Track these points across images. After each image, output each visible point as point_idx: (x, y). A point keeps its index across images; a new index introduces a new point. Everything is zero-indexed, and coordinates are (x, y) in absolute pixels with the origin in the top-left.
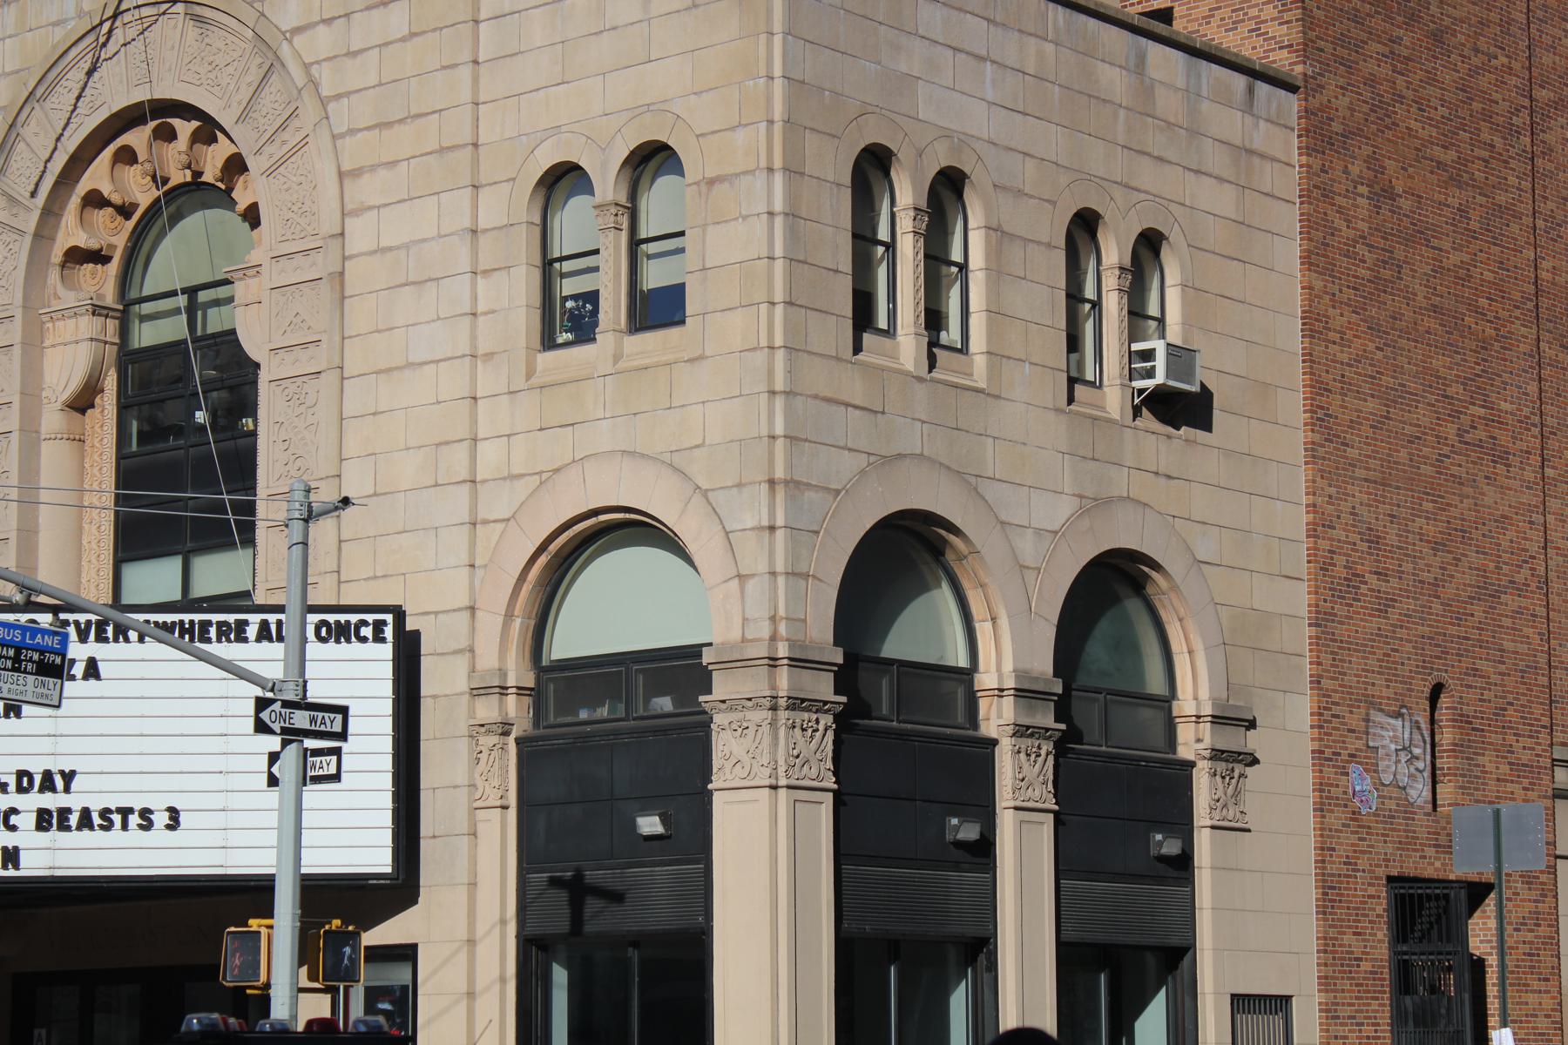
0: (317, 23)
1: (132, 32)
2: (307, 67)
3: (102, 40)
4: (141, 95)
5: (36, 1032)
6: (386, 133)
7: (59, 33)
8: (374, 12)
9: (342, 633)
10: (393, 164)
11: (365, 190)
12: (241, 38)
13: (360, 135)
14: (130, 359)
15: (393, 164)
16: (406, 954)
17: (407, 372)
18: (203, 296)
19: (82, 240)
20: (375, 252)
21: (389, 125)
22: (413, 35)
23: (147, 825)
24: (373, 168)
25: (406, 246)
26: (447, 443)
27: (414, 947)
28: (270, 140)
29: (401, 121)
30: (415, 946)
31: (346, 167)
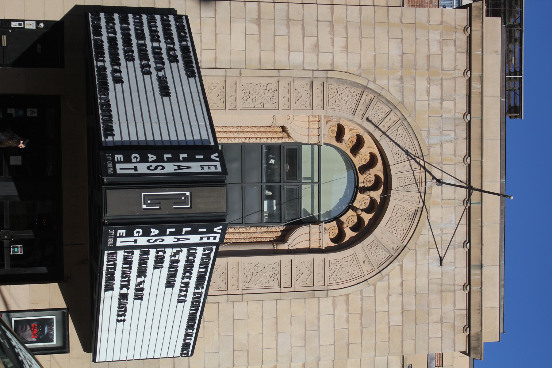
0: (402, 277)
1: (417, 175)
2: (388, 275)
3: (418, 160)
4: (394, 185)
5: (36, 110)
6: (358, 316)
7: (424, 134)
8: (400, 307)
9: (186, 346)
10: (348, 321)
11: (341, 301)
12: (403, 240)
13: (360, 302)
14: (299, 145)
15: (348, 321)
16: (64, 348)
17: (275, 333)
18: (316, 187)
19: (346, 137)
20: (319, 314)
21: (361, 319)
22: (389, 327)
23: (118, 315)
24: (348, 310)
25: (318, 330)
26: (248, 355)
27: (68, 352)
28: (366, 256)
29: (361, 323)
30: (68, 352)
31: (351, 297)
